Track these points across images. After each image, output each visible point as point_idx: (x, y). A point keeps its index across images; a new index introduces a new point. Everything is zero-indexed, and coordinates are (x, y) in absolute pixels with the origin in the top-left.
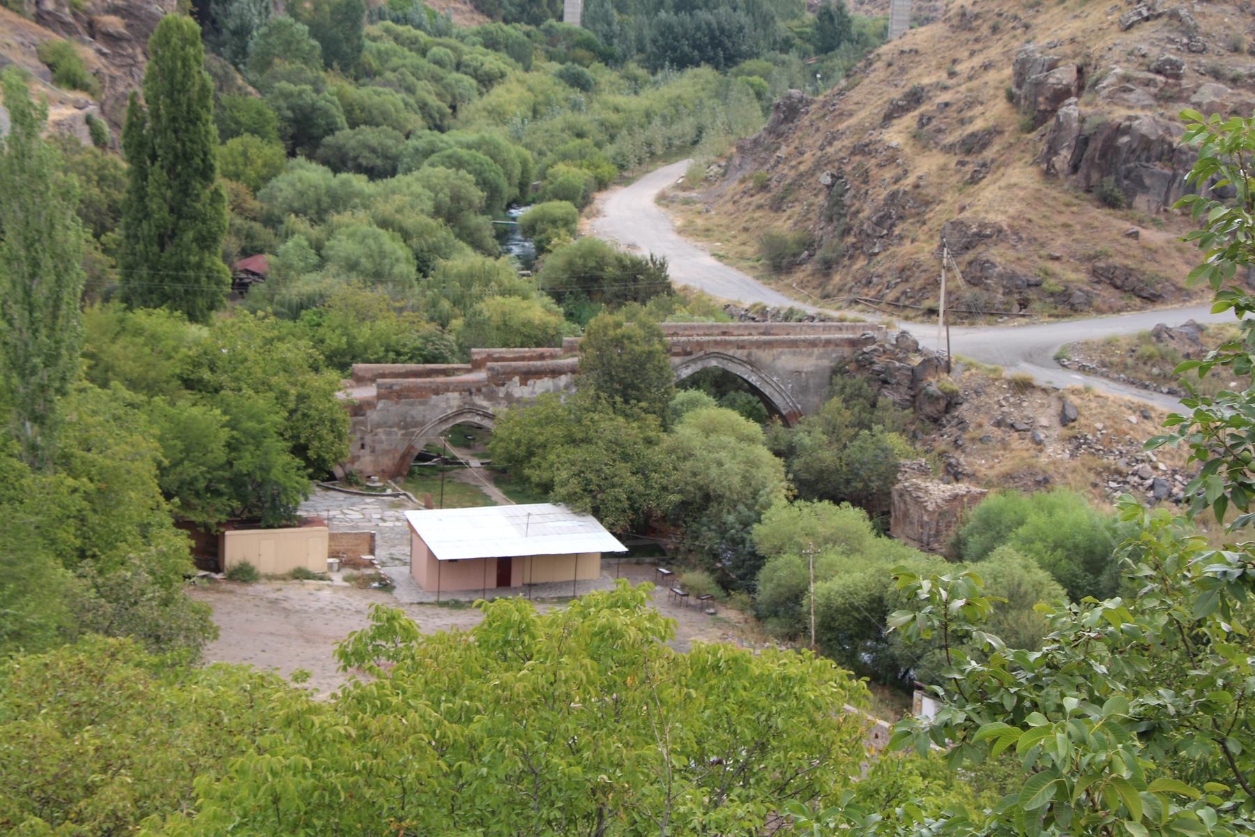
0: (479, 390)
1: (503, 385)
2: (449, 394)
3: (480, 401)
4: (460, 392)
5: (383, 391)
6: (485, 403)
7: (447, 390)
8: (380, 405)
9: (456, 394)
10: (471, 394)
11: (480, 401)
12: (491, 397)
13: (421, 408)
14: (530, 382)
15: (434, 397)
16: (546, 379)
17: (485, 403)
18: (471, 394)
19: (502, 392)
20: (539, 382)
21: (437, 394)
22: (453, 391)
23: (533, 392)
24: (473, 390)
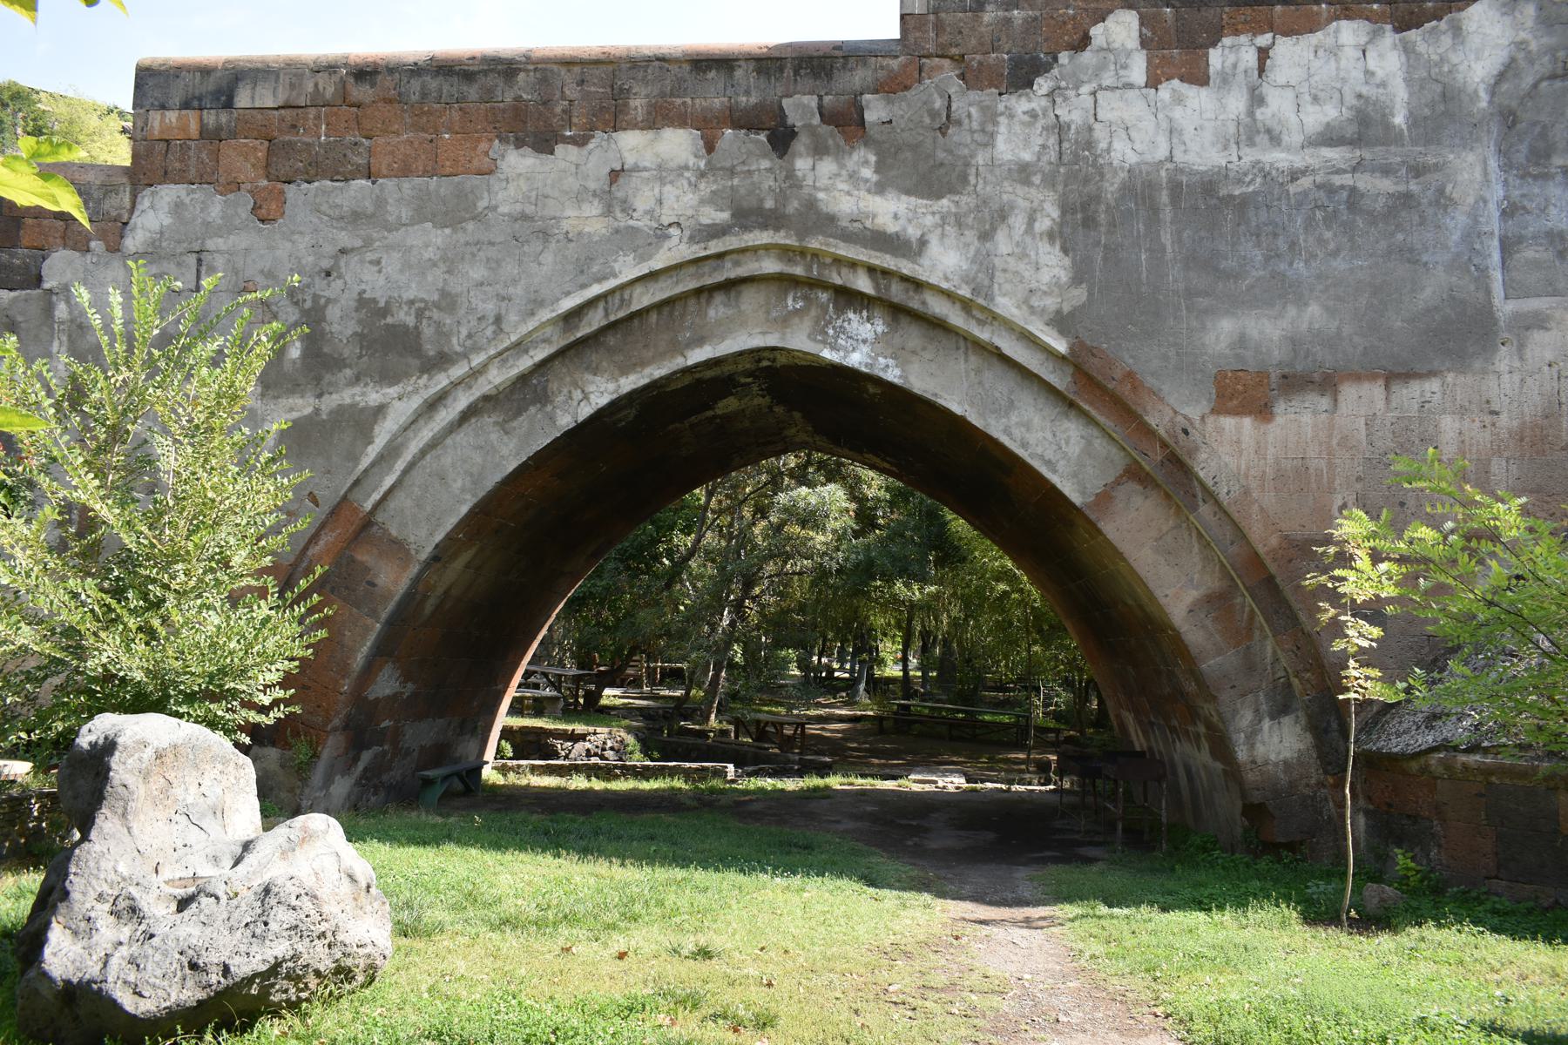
0: (846, 122)
1: (1022, 75)
2: (632, 144)
3: (847, 188)
4: (708, 127)
5: (167, 121)
6: (890, 211)
7: (612, 116)
8: (154, 214)
9: (678, 144)
10: (782, 139)
11: (849, 190)
12: (928, 170)
13: (430, 239)
14: (1231, 54)
15: (518, 162)
16: (1349, 32)
17: (890, 211)
18: (782, 139)
19: (1015, 132)
20: (1290, 54)
21: (544, 143)
22: (658, 118)
23: (1252, 131)
24: (801, 107)
